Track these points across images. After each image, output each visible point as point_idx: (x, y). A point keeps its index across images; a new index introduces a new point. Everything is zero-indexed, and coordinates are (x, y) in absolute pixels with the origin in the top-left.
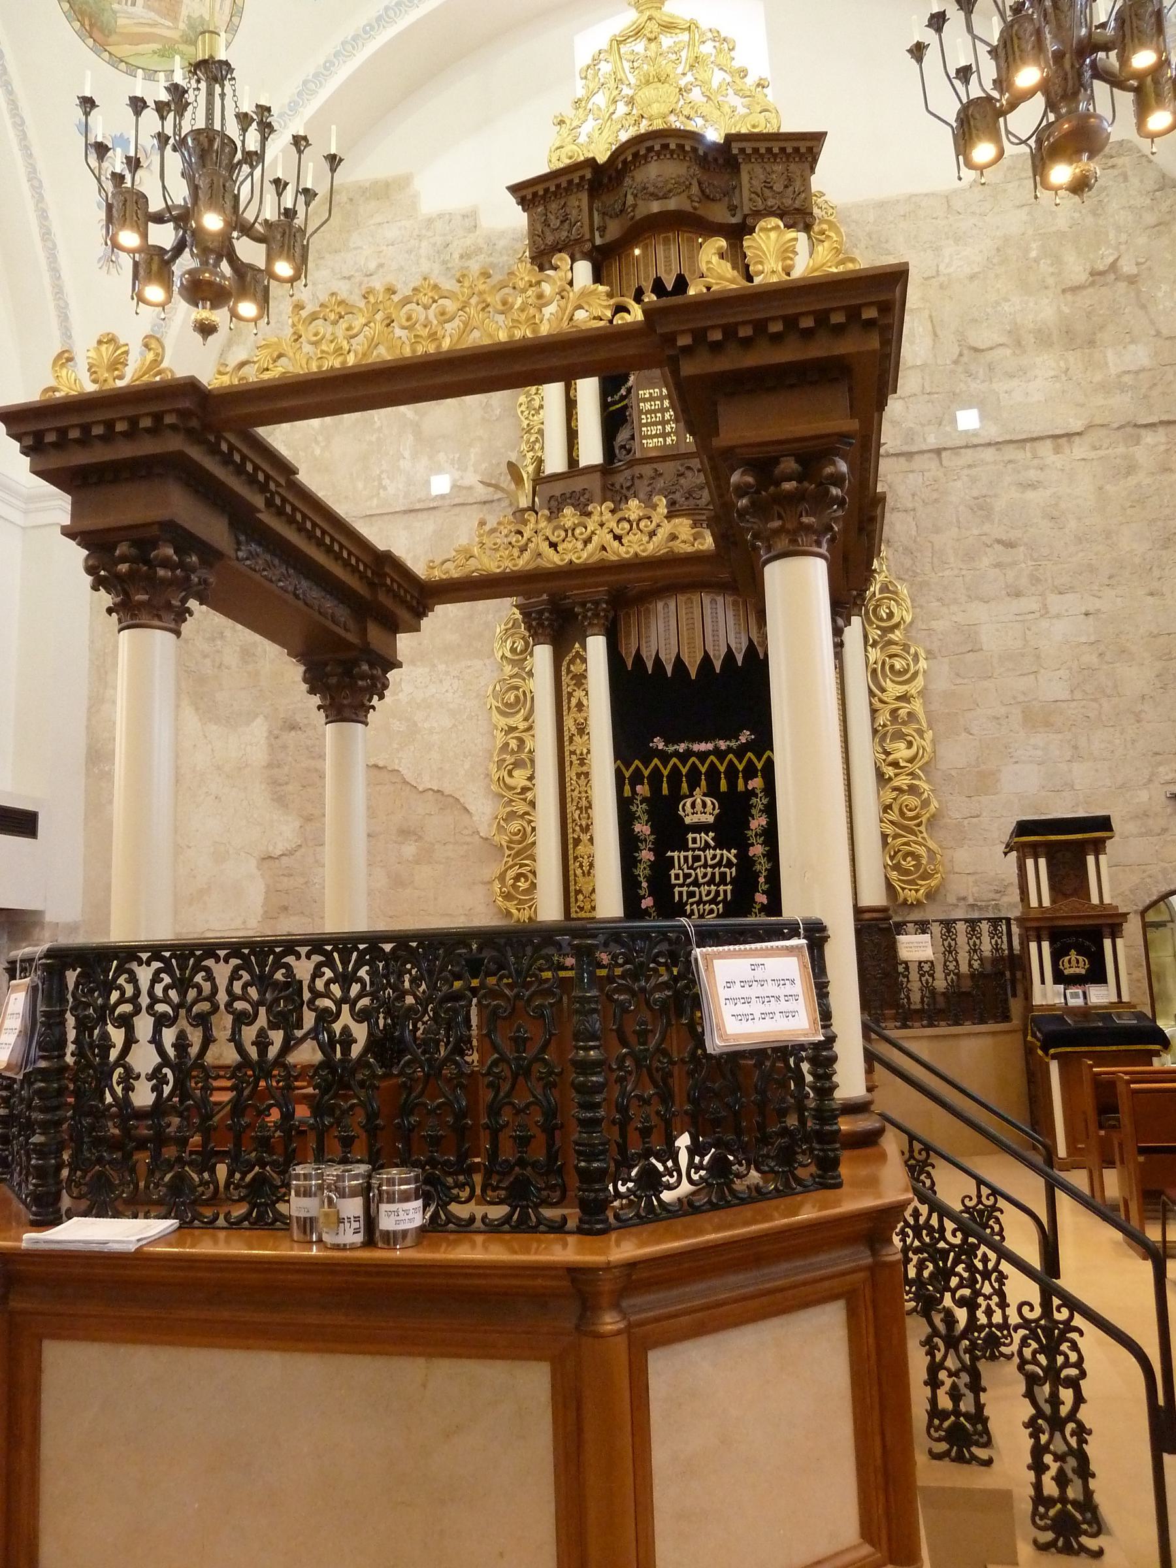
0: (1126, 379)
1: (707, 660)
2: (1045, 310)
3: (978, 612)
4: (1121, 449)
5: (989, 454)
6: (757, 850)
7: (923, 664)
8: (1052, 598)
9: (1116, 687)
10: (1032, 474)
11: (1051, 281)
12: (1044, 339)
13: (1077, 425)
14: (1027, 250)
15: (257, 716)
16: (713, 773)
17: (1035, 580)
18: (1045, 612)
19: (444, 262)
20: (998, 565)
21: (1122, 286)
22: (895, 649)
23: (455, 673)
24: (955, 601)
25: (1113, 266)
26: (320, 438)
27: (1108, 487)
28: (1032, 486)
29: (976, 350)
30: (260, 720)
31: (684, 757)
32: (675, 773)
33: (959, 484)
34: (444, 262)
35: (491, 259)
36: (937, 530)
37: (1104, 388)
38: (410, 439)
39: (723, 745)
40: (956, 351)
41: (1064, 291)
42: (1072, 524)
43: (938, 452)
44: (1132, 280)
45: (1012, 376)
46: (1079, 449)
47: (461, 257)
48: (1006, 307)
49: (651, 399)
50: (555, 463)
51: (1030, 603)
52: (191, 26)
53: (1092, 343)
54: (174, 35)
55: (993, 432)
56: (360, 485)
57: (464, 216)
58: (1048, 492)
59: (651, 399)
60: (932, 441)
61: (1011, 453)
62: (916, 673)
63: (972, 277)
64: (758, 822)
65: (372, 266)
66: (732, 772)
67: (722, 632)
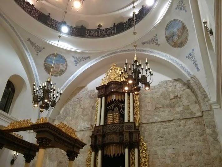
0: (179, 112)
1: (114, 155)
2: (168, 102)
3: (157, 148)
4: (179, 123)
5: (159, 124)
7: (148, 156)
8: (169, 146)
9: (178, 161)
10: (165, 127)
11: (168, 98)
12: (167, 106)
13: (172, 119)
14: (165, 94)
17: (166, 143)
18: (167, 148)
20: (160, 141)
21: (178, 99)
22: (144, 154)
23: (83, 155)
24: (153, 146)
25: (177, 95)
27: (177, 128)
28: (166, 128)
29: (157, 108)
37: (176, 114)
38: (82, 120)
40: (155, 108)
41: (170, 99)
42: (171, 134)
43: (152, 123)
44: (180, 98)
45: (162, 112)
46: (172, 123)
49: (109, 116)
51: (165, 147)
52: (60, 70)
54: (58, 71)
57: (93, 90)
58: (168, 129)
59: (109, 116)
60: (151, 121)
61: (162, 123)
62: (147, 158)
63: (157, 98)
65: (81, 97)
67: (117, 151)
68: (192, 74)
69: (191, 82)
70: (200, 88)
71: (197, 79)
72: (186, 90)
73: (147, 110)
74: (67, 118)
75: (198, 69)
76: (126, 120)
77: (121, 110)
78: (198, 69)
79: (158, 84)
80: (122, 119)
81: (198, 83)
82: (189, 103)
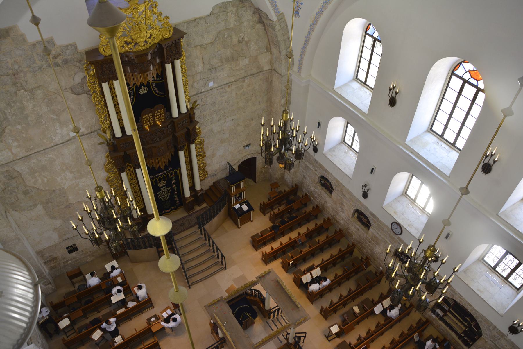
2: (228, 52)
4: (241, 84)
6: (174, 186)
11: (229, 44)
12: (227, 60)
14: (224, 36)
15: (37, 205)
16: (164, 177)
19: (47, 61)
26: (23, 131)
30: (39, 206)
31: (157, 177)
32: (156, 180)
33: (209, 99)
34: (47, 61)
35: (65, 57)
36: (204, 111)
38: (58, 124)
39: (165, 172)
46: (233, 87)
47: (53, 58)
48: (220, 53)
50: (118, 134)
53: (237, 60)
55: (216, 85)
56: (45, 141)
63: (212, 43)
64: (174, 181)
66: (168, 175)
68: (281, 10)
69: (278, 27)
70: (287, 40)
71: (286, 22)
72: (257, 27)
73: (197, 74)
74: (7, 131)
75: (296, 13)
76: (175, 114)
77: (155, 91)
78: (296, 13)
79: (211, 10)
80: (168, 114)
81: (285, 30)
82: (258, 51)
